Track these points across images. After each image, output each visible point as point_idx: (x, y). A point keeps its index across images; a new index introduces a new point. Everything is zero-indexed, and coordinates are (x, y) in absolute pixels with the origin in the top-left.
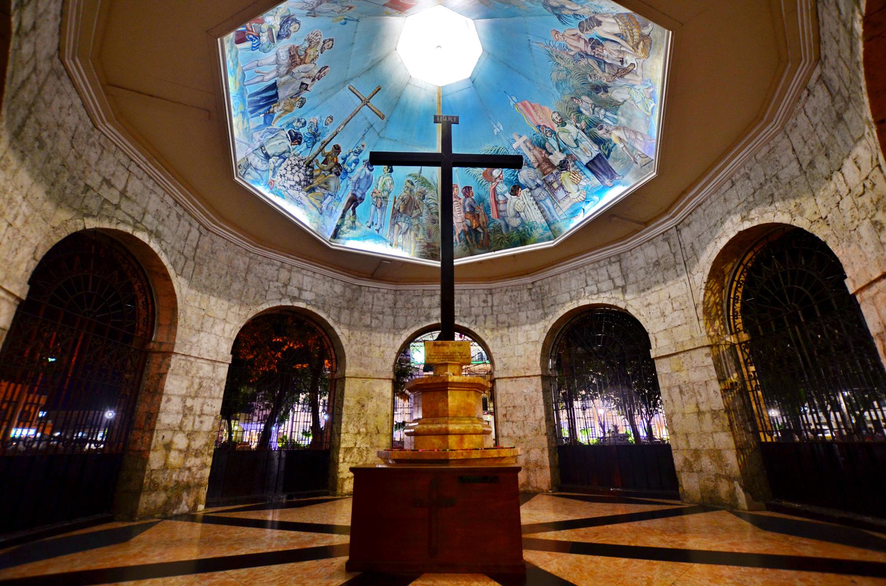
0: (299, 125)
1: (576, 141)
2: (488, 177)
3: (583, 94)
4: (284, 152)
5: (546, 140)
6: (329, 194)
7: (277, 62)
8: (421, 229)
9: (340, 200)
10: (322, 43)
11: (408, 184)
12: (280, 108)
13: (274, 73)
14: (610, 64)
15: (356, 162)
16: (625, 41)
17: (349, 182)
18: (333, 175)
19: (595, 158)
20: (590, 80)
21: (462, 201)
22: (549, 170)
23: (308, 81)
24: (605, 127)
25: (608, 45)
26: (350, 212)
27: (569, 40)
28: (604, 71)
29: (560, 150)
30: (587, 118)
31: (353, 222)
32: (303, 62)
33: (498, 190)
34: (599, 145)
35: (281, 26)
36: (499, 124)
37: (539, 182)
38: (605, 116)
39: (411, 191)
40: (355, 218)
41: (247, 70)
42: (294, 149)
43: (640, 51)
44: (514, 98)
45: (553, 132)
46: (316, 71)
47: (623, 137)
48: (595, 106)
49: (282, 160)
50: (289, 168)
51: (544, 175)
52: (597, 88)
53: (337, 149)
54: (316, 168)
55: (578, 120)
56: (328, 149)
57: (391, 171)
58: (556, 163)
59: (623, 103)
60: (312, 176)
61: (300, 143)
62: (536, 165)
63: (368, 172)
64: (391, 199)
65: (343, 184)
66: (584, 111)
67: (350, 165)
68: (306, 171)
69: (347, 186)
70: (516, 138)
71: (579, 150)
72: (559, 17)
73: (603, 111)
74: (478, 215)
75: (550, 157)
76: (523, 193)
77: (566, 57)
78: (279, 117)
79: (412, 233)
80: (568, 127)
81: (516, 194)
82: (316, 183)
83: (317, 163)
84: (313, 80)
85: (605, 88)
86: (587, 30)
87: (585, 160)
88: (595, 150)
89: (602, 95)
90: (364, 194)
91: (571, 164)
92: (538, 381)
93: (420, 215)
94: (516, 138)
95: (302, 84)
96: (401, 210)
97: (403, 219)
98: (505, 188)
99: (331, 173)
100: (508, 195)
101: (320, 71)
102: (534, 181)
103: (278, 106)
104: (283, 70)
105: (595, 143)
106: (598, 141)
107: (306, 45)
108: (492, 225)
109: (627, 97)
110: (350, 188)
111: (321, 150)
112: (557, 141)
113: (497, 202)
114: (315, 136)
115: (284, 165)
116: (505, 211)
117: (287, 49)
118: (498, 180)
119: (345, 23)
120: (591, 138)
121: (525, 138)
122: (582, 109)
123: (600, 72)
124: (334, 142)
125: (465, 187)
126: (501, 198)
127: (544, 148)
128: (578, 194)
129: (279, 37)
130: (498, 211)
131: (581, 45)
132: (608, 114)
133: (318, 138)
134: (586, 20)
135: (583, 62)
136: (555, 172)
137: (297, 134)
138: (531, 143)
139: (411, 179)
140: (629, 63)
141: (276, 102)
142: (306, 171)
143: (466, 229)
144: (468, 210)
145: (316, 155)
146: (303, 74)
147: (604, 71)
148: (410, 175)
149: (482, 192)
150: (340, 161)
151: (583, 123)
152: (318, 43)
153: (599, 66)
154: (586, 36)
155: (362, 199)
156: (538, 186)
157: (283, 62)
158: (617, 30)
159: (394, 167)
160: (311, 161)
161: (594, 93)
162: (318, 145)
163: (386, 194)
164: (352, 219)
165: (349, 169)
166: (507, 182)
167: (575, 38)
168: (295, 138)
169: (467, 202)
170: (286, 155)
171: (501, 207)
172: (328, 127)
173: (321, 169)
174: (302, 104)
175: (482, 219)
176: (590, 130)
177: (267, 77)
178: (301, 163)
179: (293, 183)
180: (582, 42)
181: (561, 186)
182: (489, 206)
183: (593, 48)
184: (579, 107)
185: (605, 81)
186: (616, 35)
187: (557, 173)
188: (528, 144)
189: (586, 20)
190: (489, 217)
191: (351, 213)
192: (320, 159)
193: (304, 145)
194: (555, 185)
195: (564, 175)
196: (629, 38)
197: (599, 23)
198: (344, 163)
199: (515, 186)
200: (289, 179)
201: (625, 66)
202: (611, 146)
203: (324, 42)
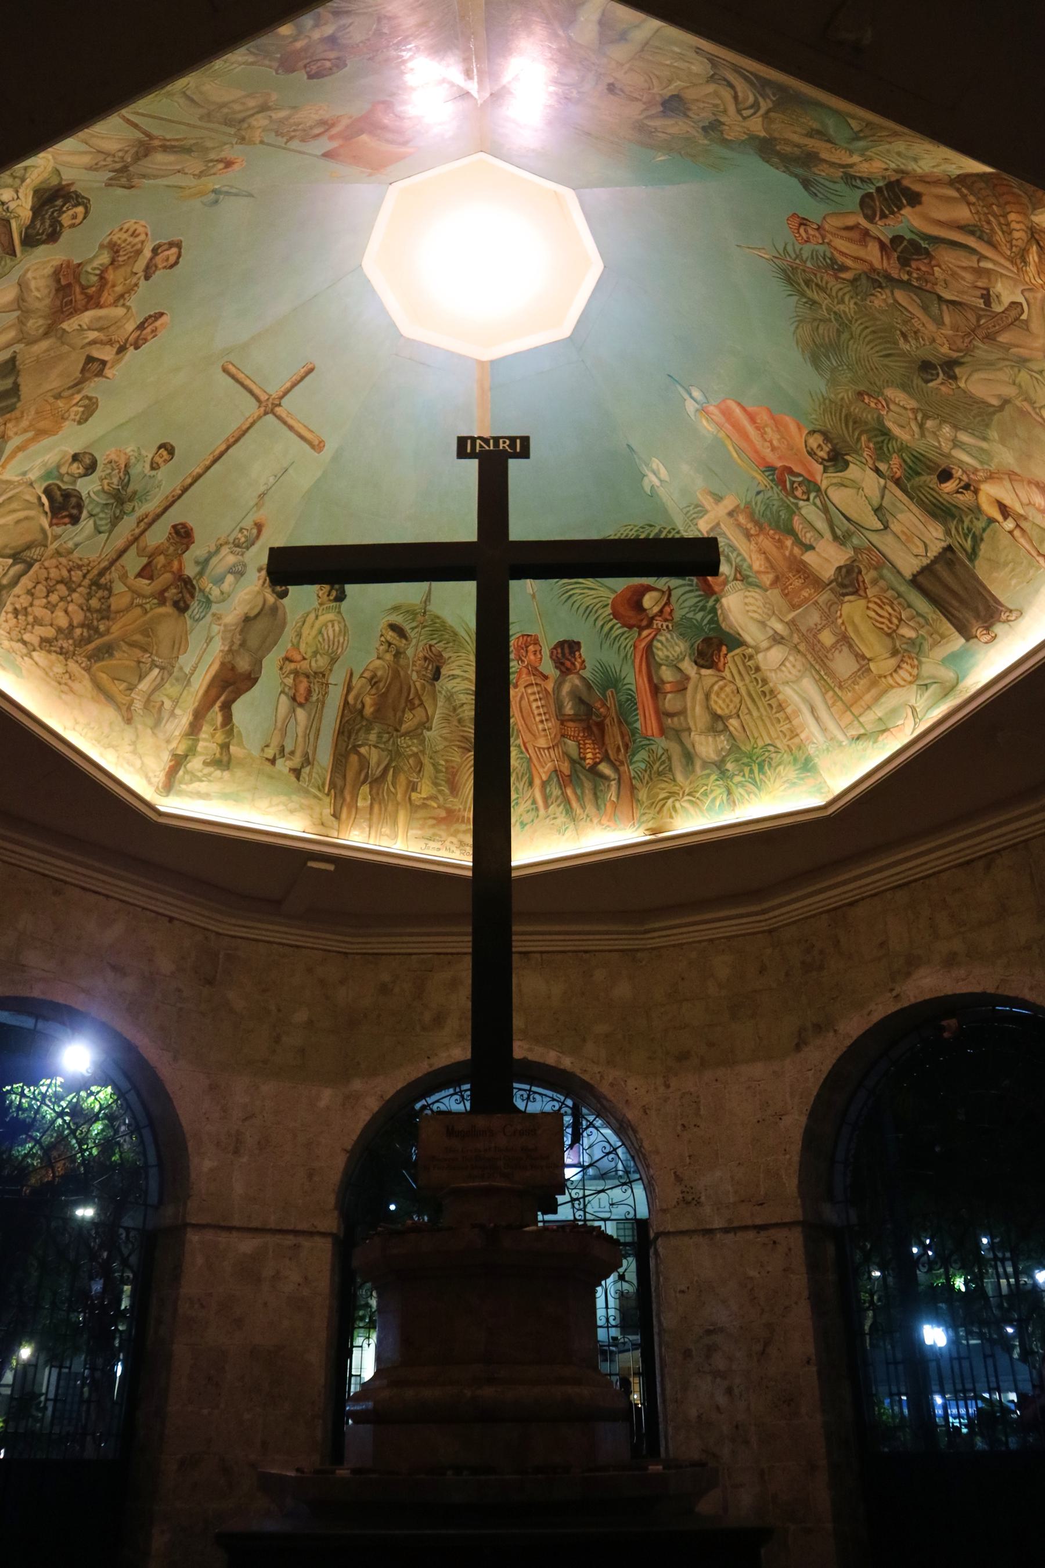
0: (76, 469)
1: (878, 510)
2: (631, 612)
3: (889, 383)
4: (29, 547)
5: (793, 511)
6: (154, 665)
7: (20, 302)
8: (428, 768)
9: (186, 681)
10: (147, 253)
11: (390, 635)
12: (24, 423)
13: (12, 334)
15: (238, 572)
17: (215, 628)
18: (168, 609)
19: (936, 560)
20: (904, 346)
21: (550, 686)
22: (805, 593)
23: (106, 354)
24: (958, 473)
25: (948, 258)
26: (216, 715)
27: (839, 243)
28: (940, 322)
29: (836, 538)
30: (903, 448)
31: (225, 747)
32: (93, 301)
33: (660, 654)
34: (944, 523)
35: (37, 211)
36: (656, 463)
37: (779, 627)
38: (956, 444)
39: (398, 654)
40: (230, 733)
42: (56, 537)
43: (1032, 269)
44: (696, 394)
45: (812, 486)
46: (130, 326)
47: (1008, 500)
48: (926, 417)
49: (19, 567)
50: (41, 589)
51: (794, 607)
52: (926, 368)
53: (183, 535)
54: (119, 588)
55: (881, 453)
56: (158, 536)
57: (341, 598)
58: (828, 573)
59: (1001, 408)
60: (106, 614)
61: (75, 520)
62: (767, 579)
63: (271, 599)
64: (337, 678)
65: (196, 639)
66: (896, 431)
67: (219, 580)
68: (89, 596)
69: (209, 640)
70: (707, 502)
71: (889, 538)
72: (806, 184)
73: (947, 429)
74: (601, 726)
75: (809, 557)
76: (731, 660)
77: (834, 286)
78: (20, 449)
79: (402, 779)
80: (853, 471)
81: (712, 665)
82: (116, 629)
83: (124, 577)
84: (122, 349)
85: (950, 366)
86: (883, 216)
87: (909, 564)
88: (935, 537)
90: (258, 664)
91: (868, 576)
92: (795, 1239)
93: (425, 724)
94: (707, 502)
95: (90, 359)
96: (369, 710)
97: (373, 737)
98: (680, 647)
99: (162, 602)
100: (688, 667)
101: (141, 327)
102: (763, 624)
103: (18, 420)
104: (35, 324)
105: (934, 515)
106: (941, 512)
107: (105, 258)
108: (643, 755)
109: (1010, 391)
110: (218, 647)
111: (136, 539)
112: (826, 510)
113: (656, 690)
114: (120, 498)
115: (26, 582)
116: (683, 712)
117: (49, 270)
118: (658, 623)
119: (216, 202)
120: (921, 504)
121: (729, 503)
122: (889, 424)
123: (931, 327)
124: (174, 516)
125: (561, 644)
126: (667, 674)
127: (791, 532)
128: (893, 662)
129: (30, 241)
130: (661, 715)
131: (873, 253)
132: (964, 437)
133: (128, 507)
134: (879, 190)
135: (880, 300)
136: (824, 597)
137: (67, 495)
138: (751, 516)
139: (397, 619)
142: (89, 596)
143: (565, 767)
144: (569, 709)
145: (121, 553)
146: (93, 335)
147: (940, 322)
148: (396, 609)
149: (611, 658)
150: (190, 571)
151: (895, 461)
152: (139, 252)
153: (925, 308)
155: (250, 680)
156: (777, 639)
157: (37, 305)
158: (963, 213)
159: (349, 588)
160: (101, 574)
161: (917, 381)
162: (127, 526)
163: (322, 662)
164: (220, 737)
165: (215, 592)
166: (685, 628)
167: (855, 235)
168: (63, 507)
169: (566, 688)
170: (35, 553)
171: (670, 702)
172: (160, 474)
173: (136, 593)
175: (614, 736)
176: (918, 480)
178: (77, 575)
179: (50, 632)
181: (844, 639)
182: (632, 700)
184: (880, 420)
185: (945, 350)
186: (962, 228)
187: (830, 604)
188: (742, 519)
189: (879, 190)
190: (634, 732)
191: (219, 719)
192: (133, 562)
193: (86, 525)
194: (827, 638)
195: (853, 609)
197: (915, 199)
198: (201, 574)
199: (707, 641)
200: (38, 622)
202: (980, 524)
203: (155, 251)
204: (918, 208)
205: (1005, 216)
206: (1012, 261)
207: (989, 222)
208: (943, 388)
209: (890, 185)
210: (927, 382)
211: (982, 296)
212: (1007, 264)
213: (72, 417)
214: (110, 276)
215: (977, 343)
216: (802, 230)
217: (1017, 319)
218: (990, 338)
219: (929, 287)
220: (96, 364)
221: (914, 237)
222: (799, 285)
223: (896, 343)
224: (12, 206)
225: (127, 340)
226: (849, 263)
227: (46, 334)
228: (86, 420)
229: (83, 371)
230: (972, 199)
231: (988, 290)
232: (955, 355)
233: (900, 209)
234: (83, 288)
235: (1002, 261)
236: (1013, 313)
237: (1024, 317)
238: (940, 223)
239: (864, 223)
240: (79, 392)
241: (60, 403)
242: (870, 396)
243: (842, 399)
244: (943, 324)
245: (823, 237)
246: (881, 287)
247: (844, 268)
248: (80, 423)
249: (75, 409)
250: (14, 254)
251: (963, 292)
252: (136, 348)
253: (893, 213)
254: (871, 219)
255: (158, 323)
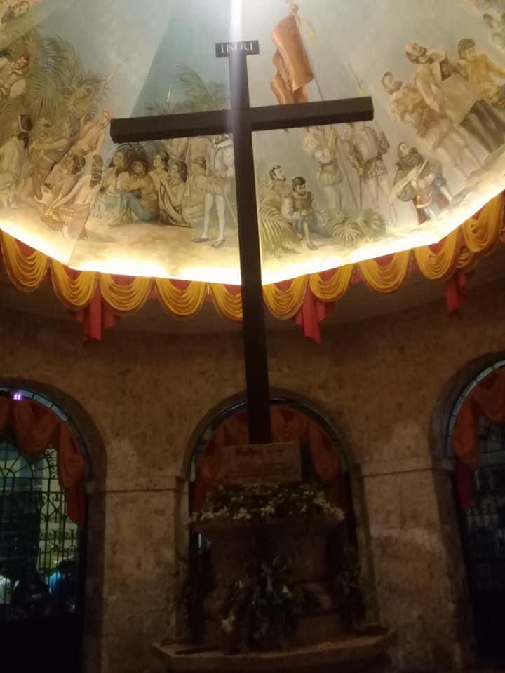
3: (28, 87)
7: (440, 143)
12: (487, 85)
13: (455, 137)
14: (52, 168)
16: (66, 204)
20: (44, 121)
28: (47, 153)
32: (422, 105)
35: (410, 167)
41: (465, 175)
43: (51, 214)
52: (29, 124)
85: (25, 139)
86: (93, 165)
89: (17, 124)
95: (444, 77)
101: (417, 61)
103: (485, 91)
104: (444, 125)
123: (47, 147)
135: (66, 127)
140: (44, 194)
141: (482, 102)
146: (434, 88)
147: (47, 153)
154: (89, 158)
174: (467, 44)
177: (461, 142)
180: (86, 148)
183: (75, 158)
185: (34, 144)
196: (66, 209)
197: (93, 184)
201: (43, 188)
203: (391, 92)
204: (89, 184)
205: (72, 216)
206: (57, 208)
207: (73, 208)
208: (15, 124)
209: (100, 177)
210: (22, 116)
211: (49, 185)
212: (56, 206)
213: (472, 54)
214: (410, 108)
215: (31, 166)
216: (106, 115)
217: (36, 194)
218: (32, 175)
219: (62, 161)
220: (444, 69)
221: (82, 172)
222: (91, 84)
223: (46, 117)
224: (415, 178)
225: (426, 63)
226: (86, 127)
227: (444, 116)
228: (470, 41)
229: (449, 75)
230: (82, 208)
231: (51, 189)
232: (30, 148)
233: (93, 175)
234: (421, 115)
235: (59, 204)
236: (38, 193)
237: (35, 197)
238: (81, 188)
239: (96, 152)
240: (459, 65)
241: (469, 71)
242: (26, 64)
243: (29, 41)
244: (46, 154)
245: (100, 124)
246: (71, 135)
247: (86, 121)
248: (474, 45)
249: (469, 58)
250: (427, 163)
251: (54, 176)
252: (425, 50)
253: (93, 170)
254: (95, 157)
255: (410, 50)
